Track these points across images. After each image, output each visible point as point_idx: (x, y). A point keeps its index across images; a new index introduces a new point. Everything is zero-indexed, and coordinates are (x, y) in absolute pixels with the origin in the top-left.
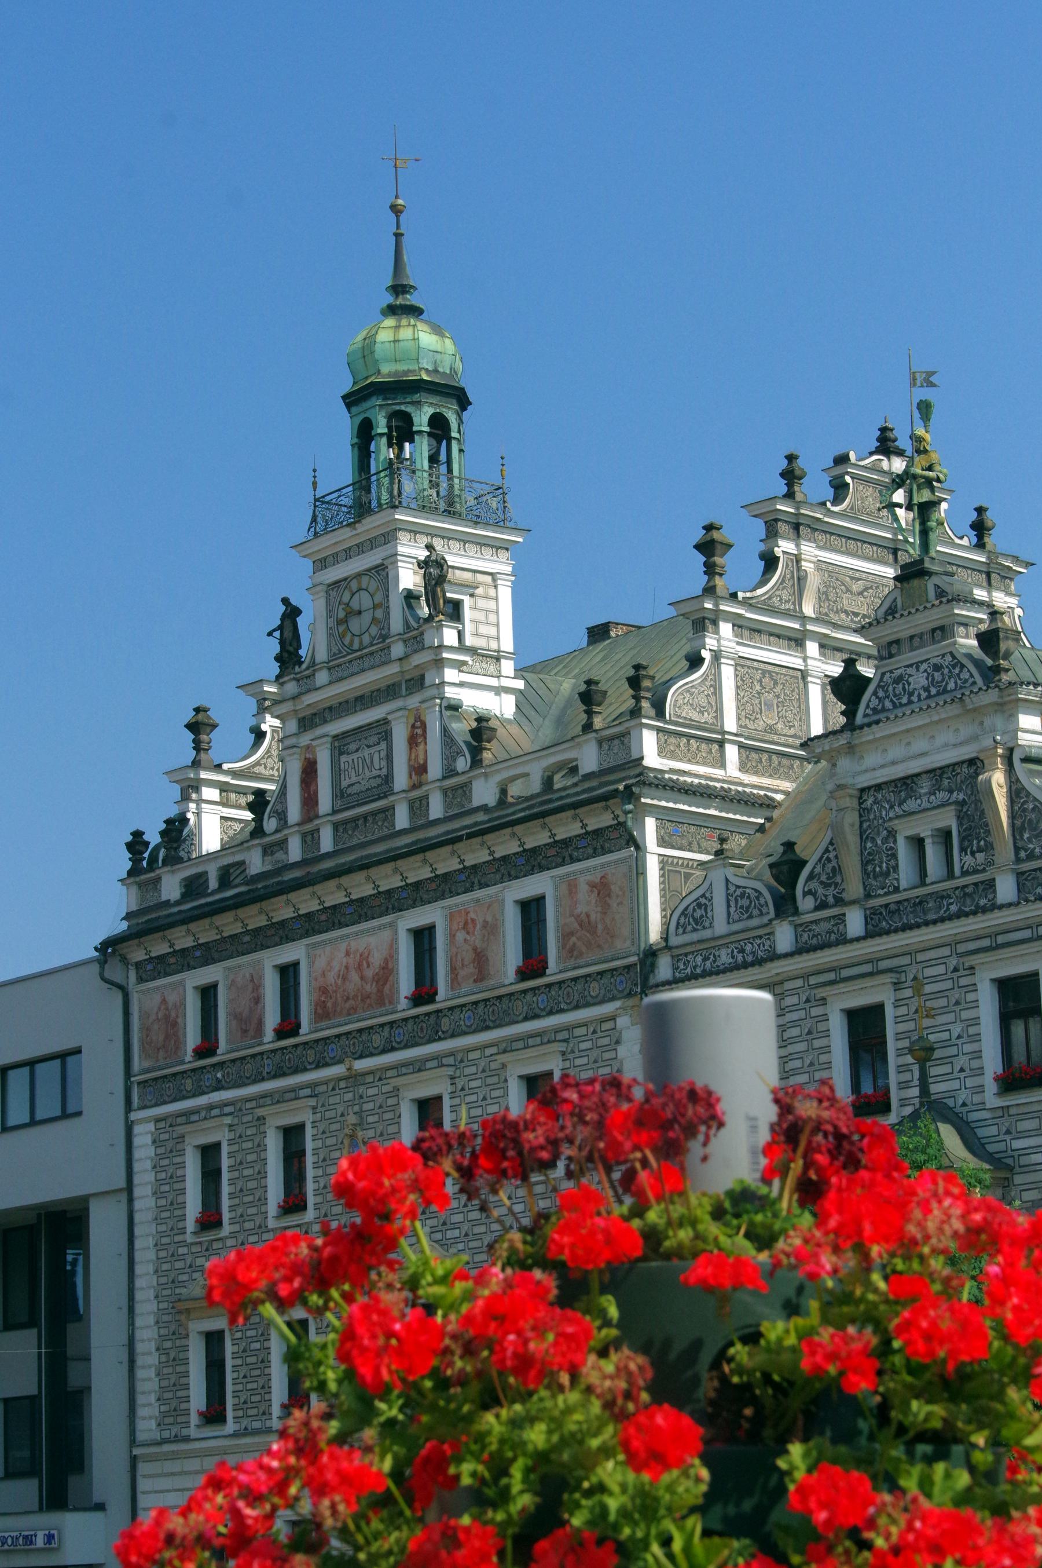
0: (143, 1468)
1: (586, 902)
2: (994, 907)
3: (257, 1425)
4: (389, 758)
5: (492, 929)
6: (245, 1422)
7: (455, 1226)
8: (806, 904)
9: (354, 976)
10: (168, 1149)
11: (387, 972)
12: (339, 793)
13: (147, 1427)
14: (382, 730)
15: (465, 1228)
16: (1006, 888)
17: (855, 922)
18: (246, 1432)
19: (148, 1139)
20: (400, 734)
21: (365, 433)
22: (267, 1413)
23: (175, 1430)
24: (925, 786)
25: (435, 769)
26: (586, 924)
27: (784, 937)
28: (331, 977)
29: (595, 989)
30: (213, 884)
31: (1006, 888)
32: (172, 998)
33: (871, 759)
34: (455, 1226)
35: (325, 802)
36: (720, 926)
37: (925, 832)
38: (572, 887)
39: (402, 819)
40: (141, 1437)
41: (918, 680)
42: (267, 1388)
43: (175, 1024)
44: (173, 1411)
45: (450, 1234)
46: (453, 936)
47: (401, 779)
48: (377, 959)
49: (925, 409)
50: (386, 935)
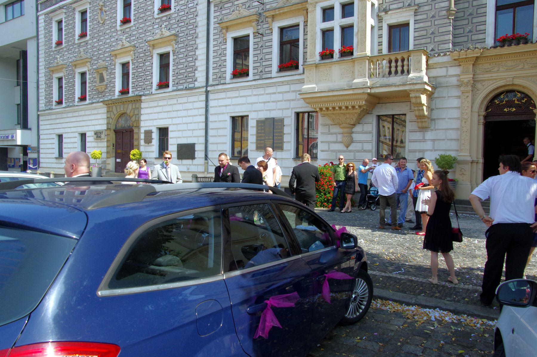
0: (41, 118)
3: (71, 104)
6: (68, 104)
7: (134, 35)
10: (48, 23)
13: (42, 106)
15: (137, 36)
18: (68, 107)
19: (43, 21)
22: (74, 101)
23: (49, 107)
34: (134, 35)
40: (40, 109)
42: (74, 93)
44: (49, 102)
45: (132, 38)
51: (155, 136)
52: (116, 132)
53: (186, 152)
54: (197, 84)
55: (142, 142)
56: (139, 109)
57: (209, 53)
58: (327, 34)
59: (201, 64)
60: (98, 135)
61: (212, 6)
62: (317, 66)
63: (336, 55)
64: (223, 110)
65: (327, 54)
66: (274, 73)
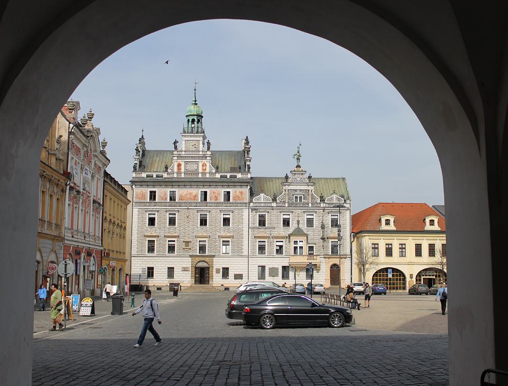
1: (238, 194)
2: (309, 207)
4: (198, 167)
5: (219, 194)
8: (278, 201)
9: (189, 195)
11: (196, 196)
12: (185, 169)
14: (197, 163)
16: (310, 205)
17: (287, 205)
20: (200, 164)
21: (193, 121)
24: (298, 191)
25: (208, 170)
26: (238, 197)
27: (274, 205)
28: (183, 194)
29: (239, 205)
30: (155, 176)
31: (310, 205)
32: (144, 191)
33: (290, 187)
35: (183, 170)
36: (262, 201)
37: (298, 196)
38: (236, 192)
39: (200, 176)
41: (299, 179)
43: (144, 195)
46: (211, 194)
47: (200, 170)
48: (194, 194)
49: (298, 148)
50: (196, 191)
51: (221, 270)
52: (196, 268)
53: (238, 277)
54: (243, 254)
55: (214, 273)
56: (213, 260)
57: (248, 244)
58: (295, 248)
59: (245, 247)
60: (185, 269)
61: (250, 229)
62: (293, 256)
63: (298, 254)
64: (255, 263)
65: (295, 252)
66: (275, 254)
